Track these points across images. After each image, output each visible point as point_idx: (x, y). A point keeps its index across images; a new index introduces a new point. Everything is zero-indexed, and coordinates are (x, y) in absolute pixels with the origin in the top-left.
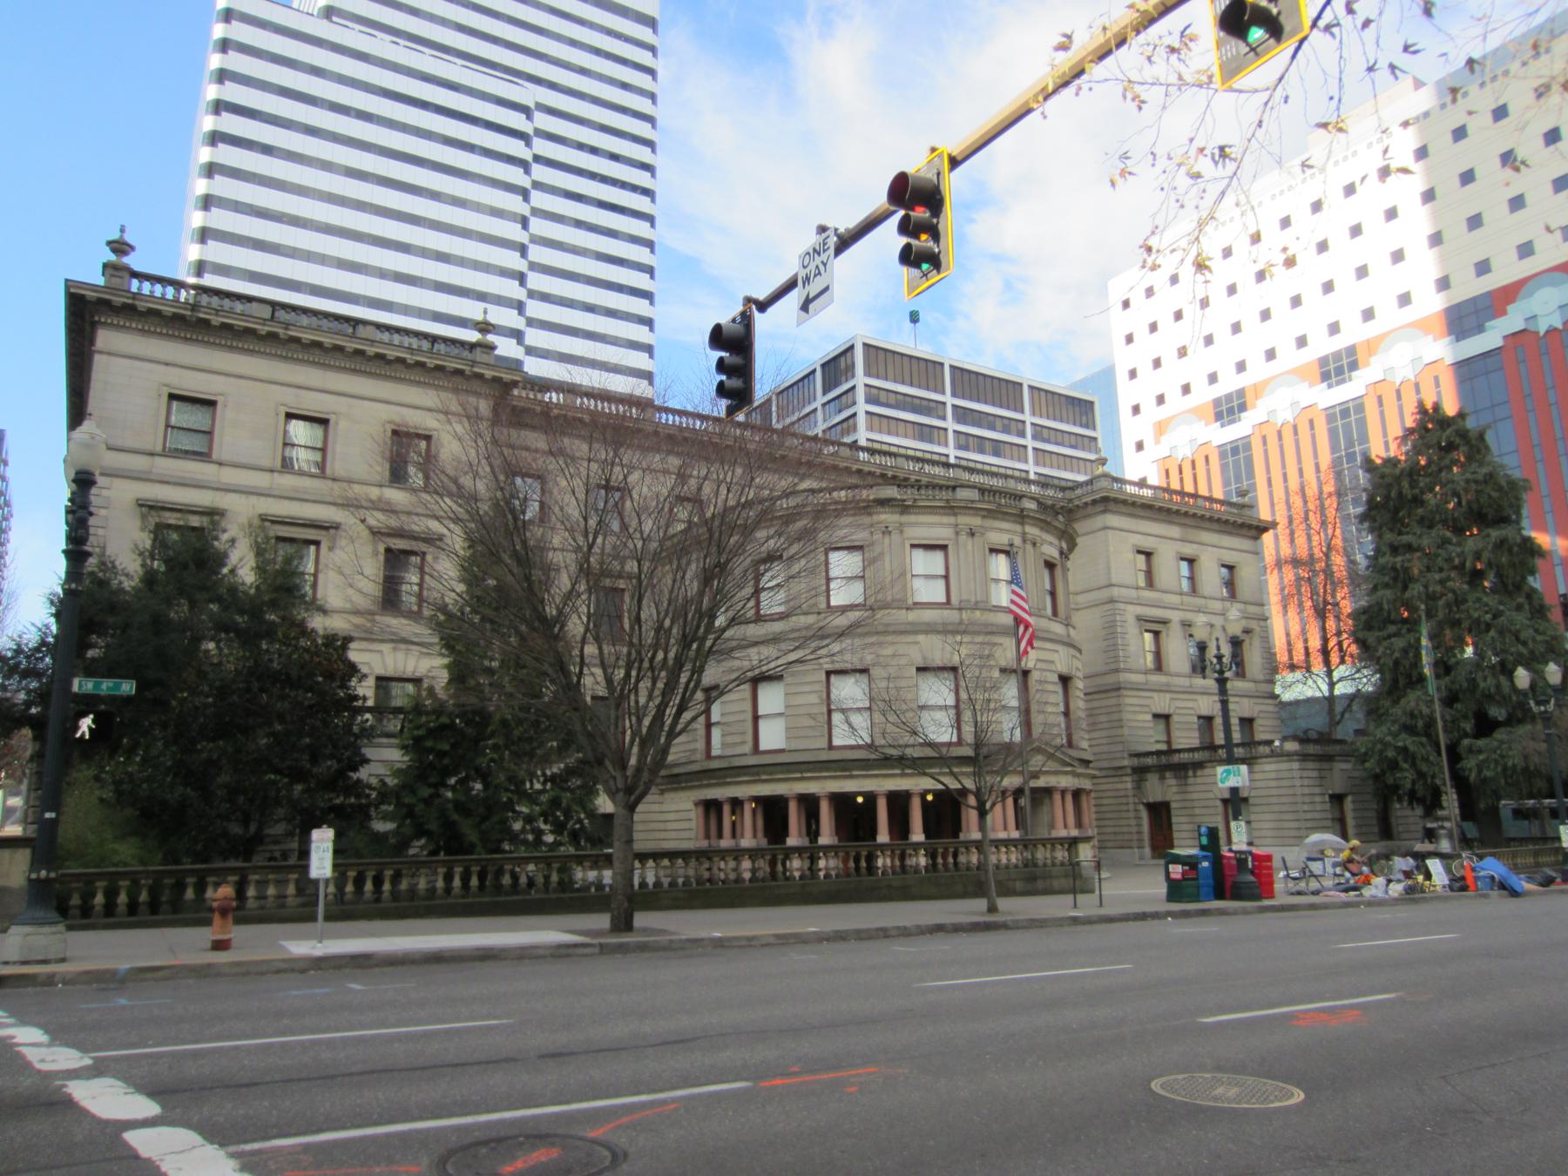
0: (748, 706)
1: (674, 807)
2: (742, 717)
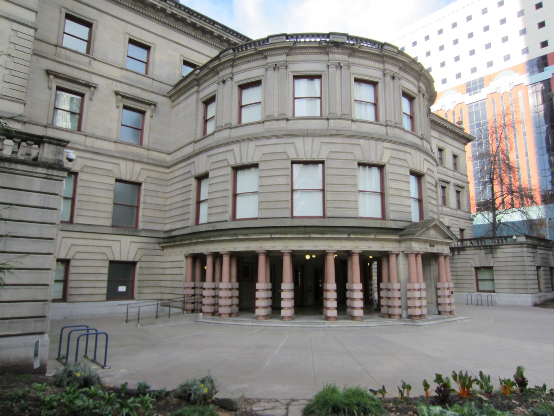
0: (230, 186)
1: (171, 259)
2: (225, 194)
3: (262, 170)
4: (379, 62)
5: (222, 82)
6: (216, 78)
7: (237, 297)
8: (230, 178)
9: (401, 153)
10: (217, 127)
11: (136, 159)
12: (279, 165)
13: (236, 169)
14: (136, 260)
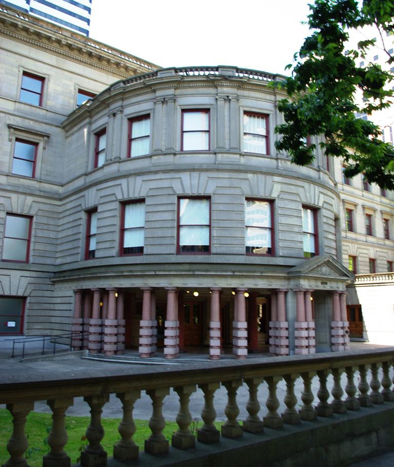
0: (117, 221)
1: (60, 294)
2: (112, 229)
3: (148, 205)
4: (270, 93)
5: (112, 115)
6: (106, 111)
7: (124, 334)
8: (117, 213)
9: (293, 187)
10: (106, 161)
11: (28, 191)
12: (165, 200)
13: (125, 204)
14: (25, 295)
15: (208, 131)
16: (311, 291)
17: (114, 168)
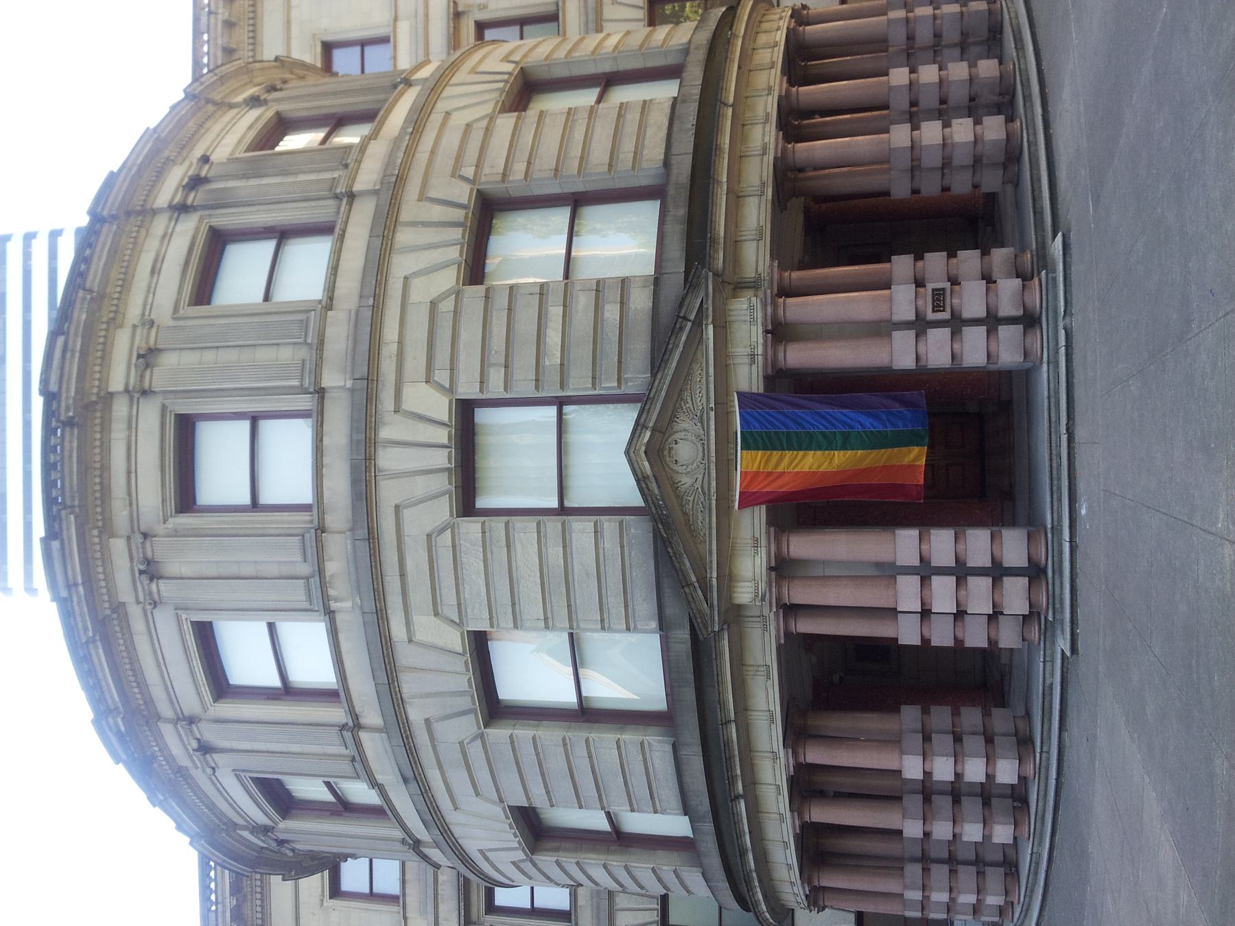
0: (550, 735)
2: (580, 752)
3: (491, 618)
8: (524, 733)
10: (358, 777)
12: (473, 562)
15: (255, 419)
16: (785, 85)
17: (374, 746)
